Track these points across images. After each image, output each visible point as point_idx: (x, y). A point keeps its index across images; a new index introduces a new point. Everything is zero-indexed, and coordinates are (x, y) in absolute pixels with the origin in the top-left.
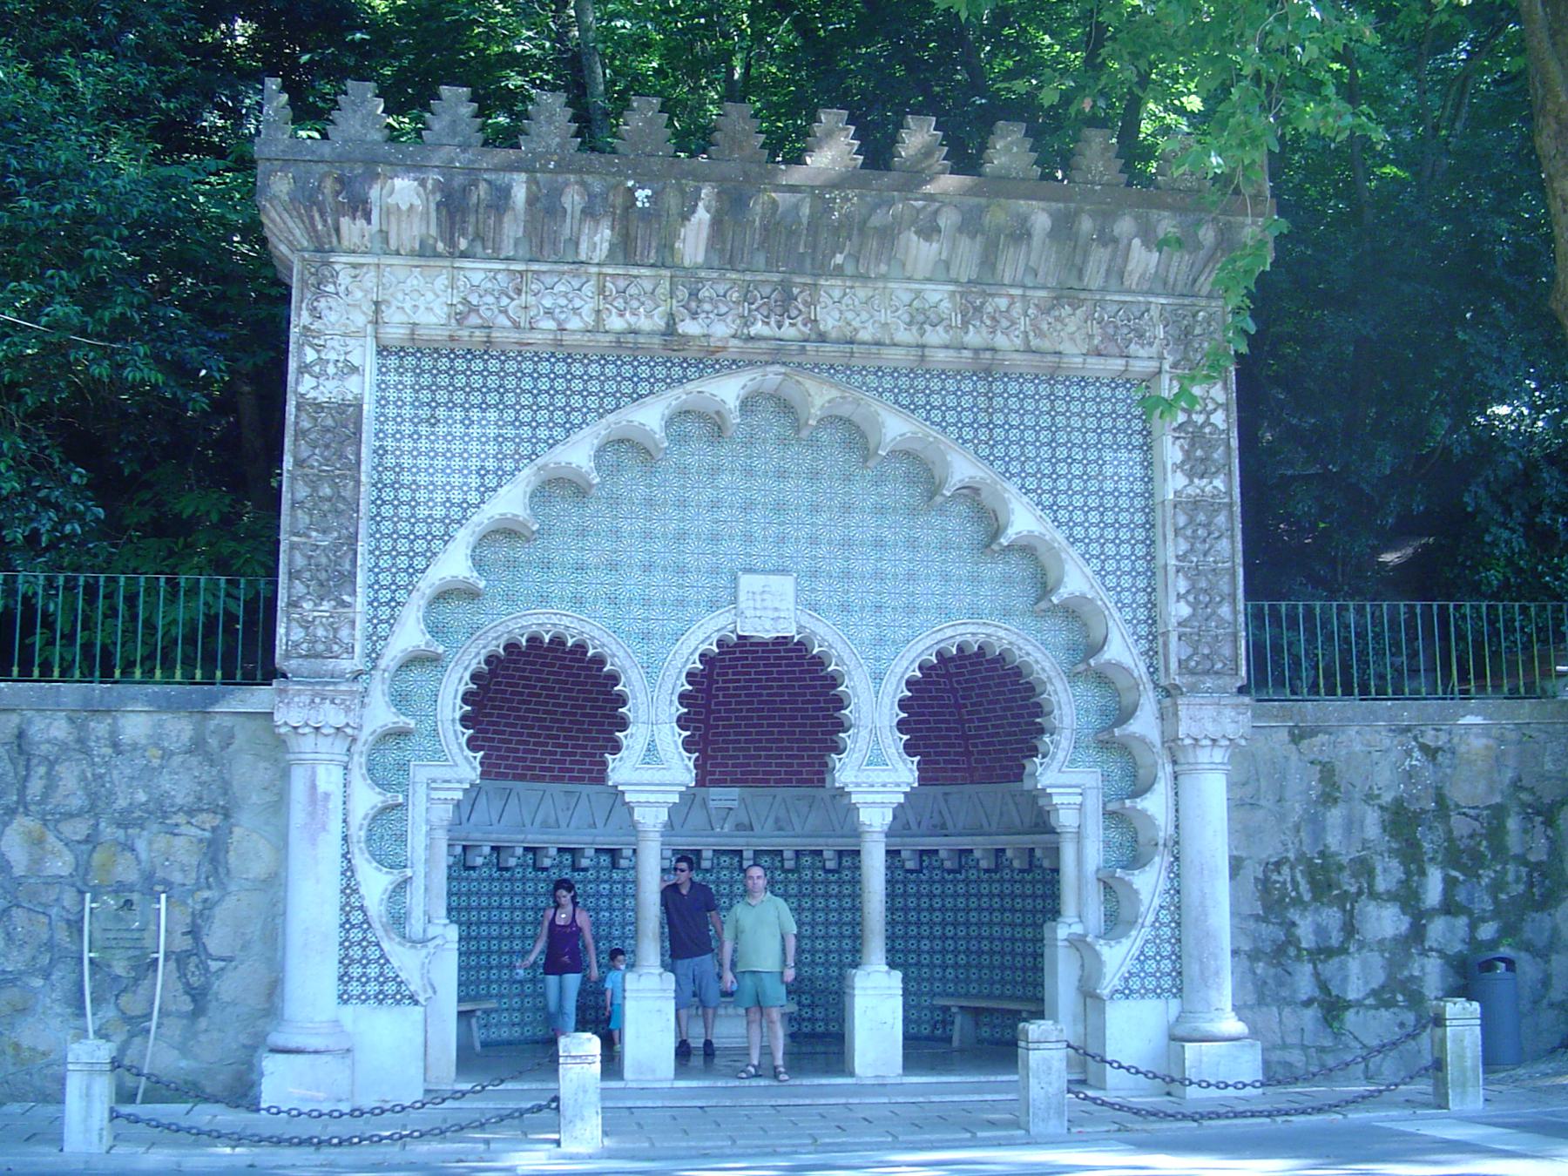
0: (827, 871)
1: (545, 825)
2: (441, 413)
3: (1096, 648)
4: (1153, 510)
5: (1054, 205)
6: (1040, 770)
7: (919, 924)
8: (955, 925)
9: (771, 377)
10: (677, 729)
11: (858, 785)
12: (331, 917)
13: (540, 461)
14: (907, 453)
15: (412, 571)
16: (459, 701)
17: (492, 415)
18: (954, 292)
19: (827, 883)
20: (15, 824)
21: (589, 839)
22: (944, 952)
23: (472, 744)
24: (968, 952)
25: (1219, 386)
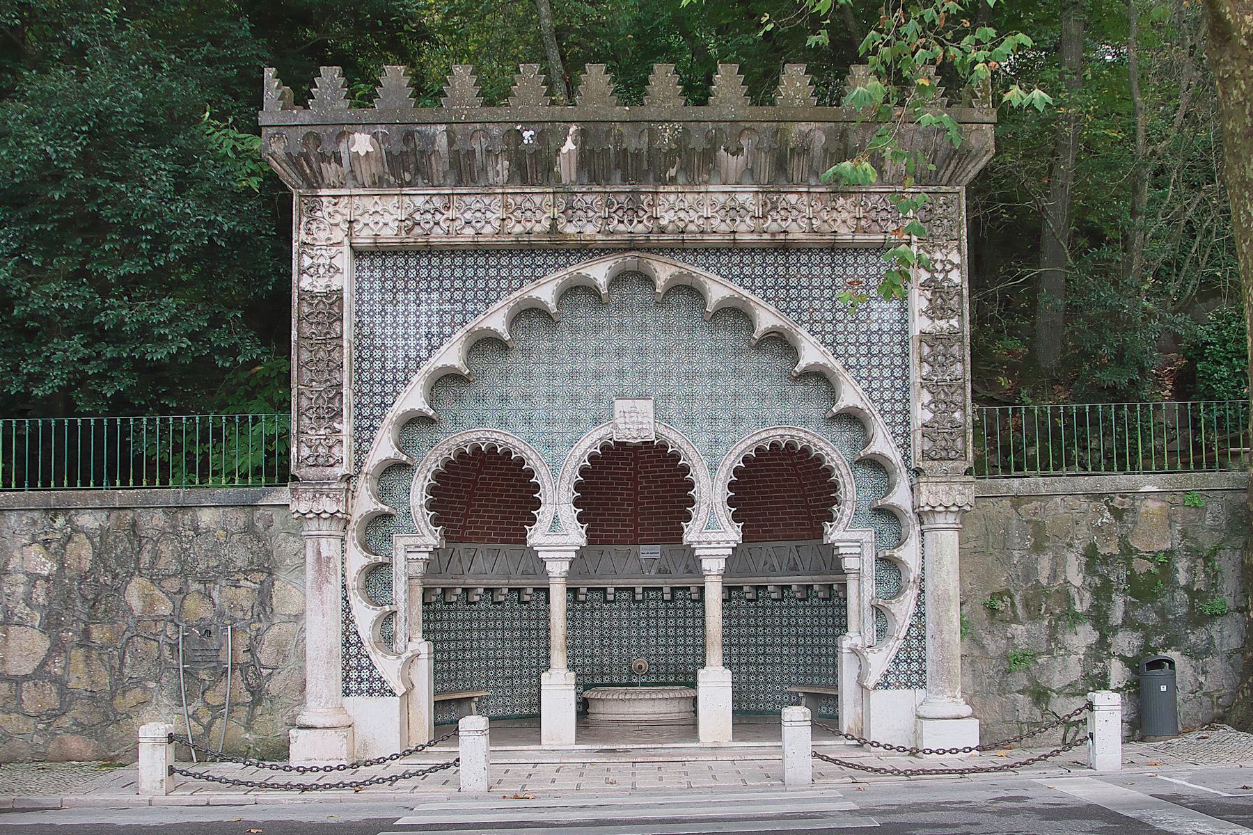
2: (400, 296)
3: (867, 443)
4: (908, 343)
5: (828, 125)
6: (830, 530)
9: (630, 259)
10: (573, 508)
11: (699, 542)
12: (334, 639)
13: (468, 327)
14: (733, 309)
15: (384, 406)
16: (424, 493)
17: (435, 296)
18: (757, 192)
20: (133, 583)
23: (436, 522)
25: (955, 251)
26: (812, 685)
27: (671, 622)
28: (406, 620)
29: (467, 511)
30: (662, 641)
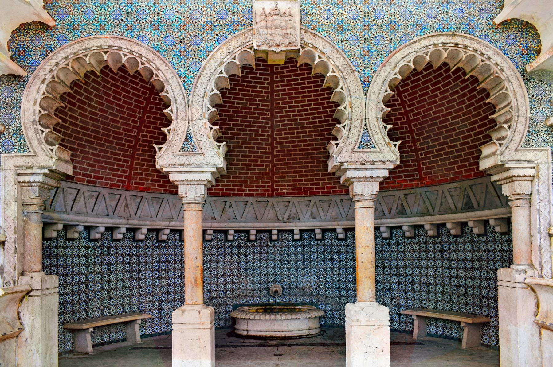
7: (391, 268)
8: (412, 268)
16: (38, 108)
19: (339, 246)
22: (405, 283)
24: (420, 283)
26: (420, 308)
27: (300, 256)
28: (16, 252)
29: (132, 164)
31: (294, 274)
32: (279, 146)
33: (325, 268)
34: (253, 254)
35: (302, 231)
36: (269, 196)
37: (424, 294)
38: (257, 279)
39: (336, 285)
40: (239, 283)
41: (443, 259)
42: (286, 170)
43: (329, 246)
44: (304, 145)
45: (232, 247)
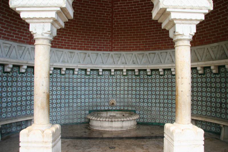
0: (148, 75)
1: (63, 62)
19: (148, 79)
21: (76, 65)
30: (122, 92)
31: (123, 94)
32: (116, 23)
33: (140, 91)
34: (101, 83)
35: (127, 70)
36: (110, 51)
37: (195, 106)
38: (103, 96)
39: (146, 101)
40: (93, 98)
41: (207, 87)
42: (120, 37)
43: (142, 79)
44: (130, 23)
45: (89, 79)
